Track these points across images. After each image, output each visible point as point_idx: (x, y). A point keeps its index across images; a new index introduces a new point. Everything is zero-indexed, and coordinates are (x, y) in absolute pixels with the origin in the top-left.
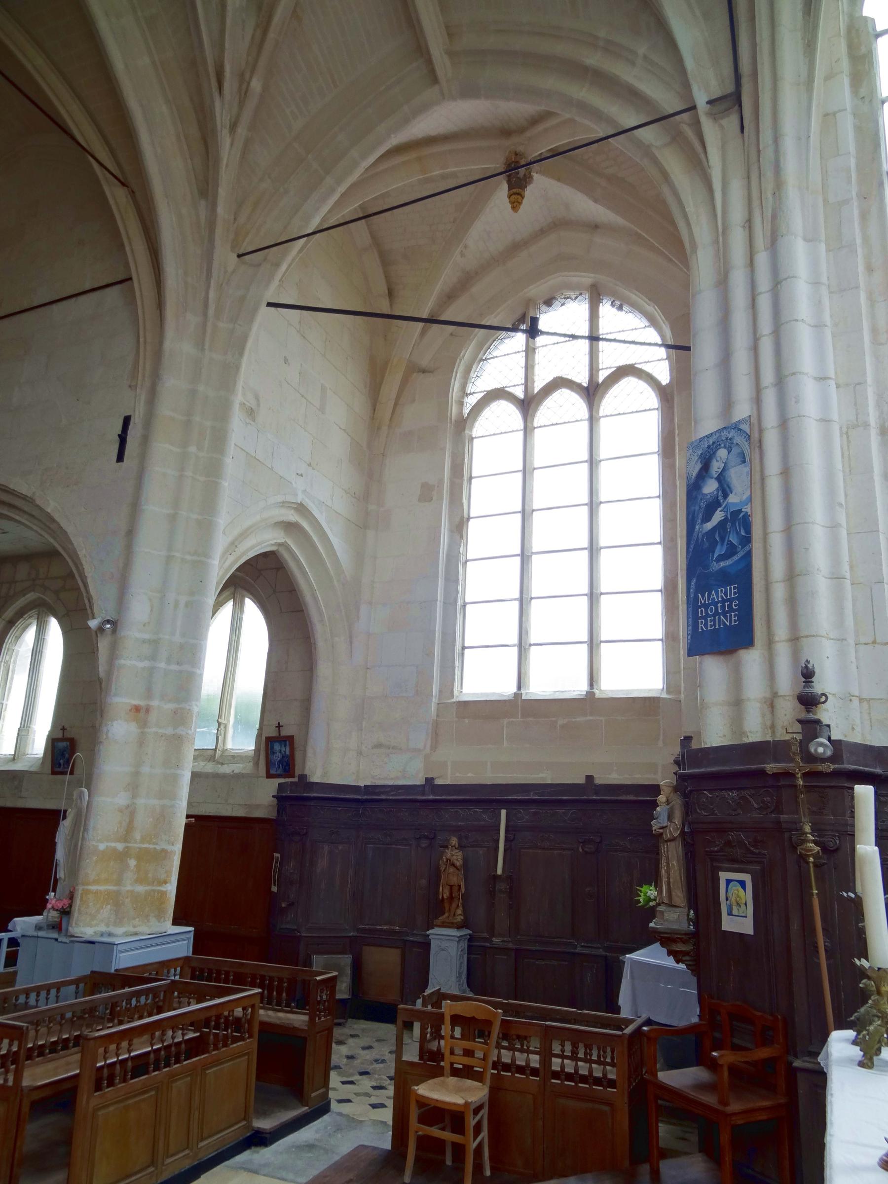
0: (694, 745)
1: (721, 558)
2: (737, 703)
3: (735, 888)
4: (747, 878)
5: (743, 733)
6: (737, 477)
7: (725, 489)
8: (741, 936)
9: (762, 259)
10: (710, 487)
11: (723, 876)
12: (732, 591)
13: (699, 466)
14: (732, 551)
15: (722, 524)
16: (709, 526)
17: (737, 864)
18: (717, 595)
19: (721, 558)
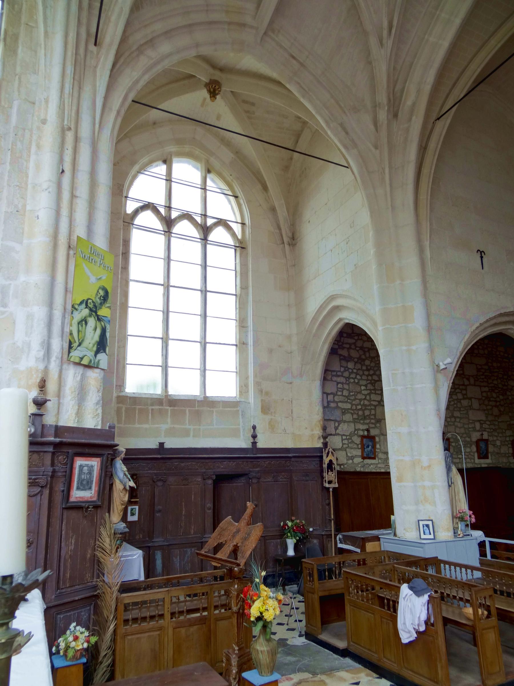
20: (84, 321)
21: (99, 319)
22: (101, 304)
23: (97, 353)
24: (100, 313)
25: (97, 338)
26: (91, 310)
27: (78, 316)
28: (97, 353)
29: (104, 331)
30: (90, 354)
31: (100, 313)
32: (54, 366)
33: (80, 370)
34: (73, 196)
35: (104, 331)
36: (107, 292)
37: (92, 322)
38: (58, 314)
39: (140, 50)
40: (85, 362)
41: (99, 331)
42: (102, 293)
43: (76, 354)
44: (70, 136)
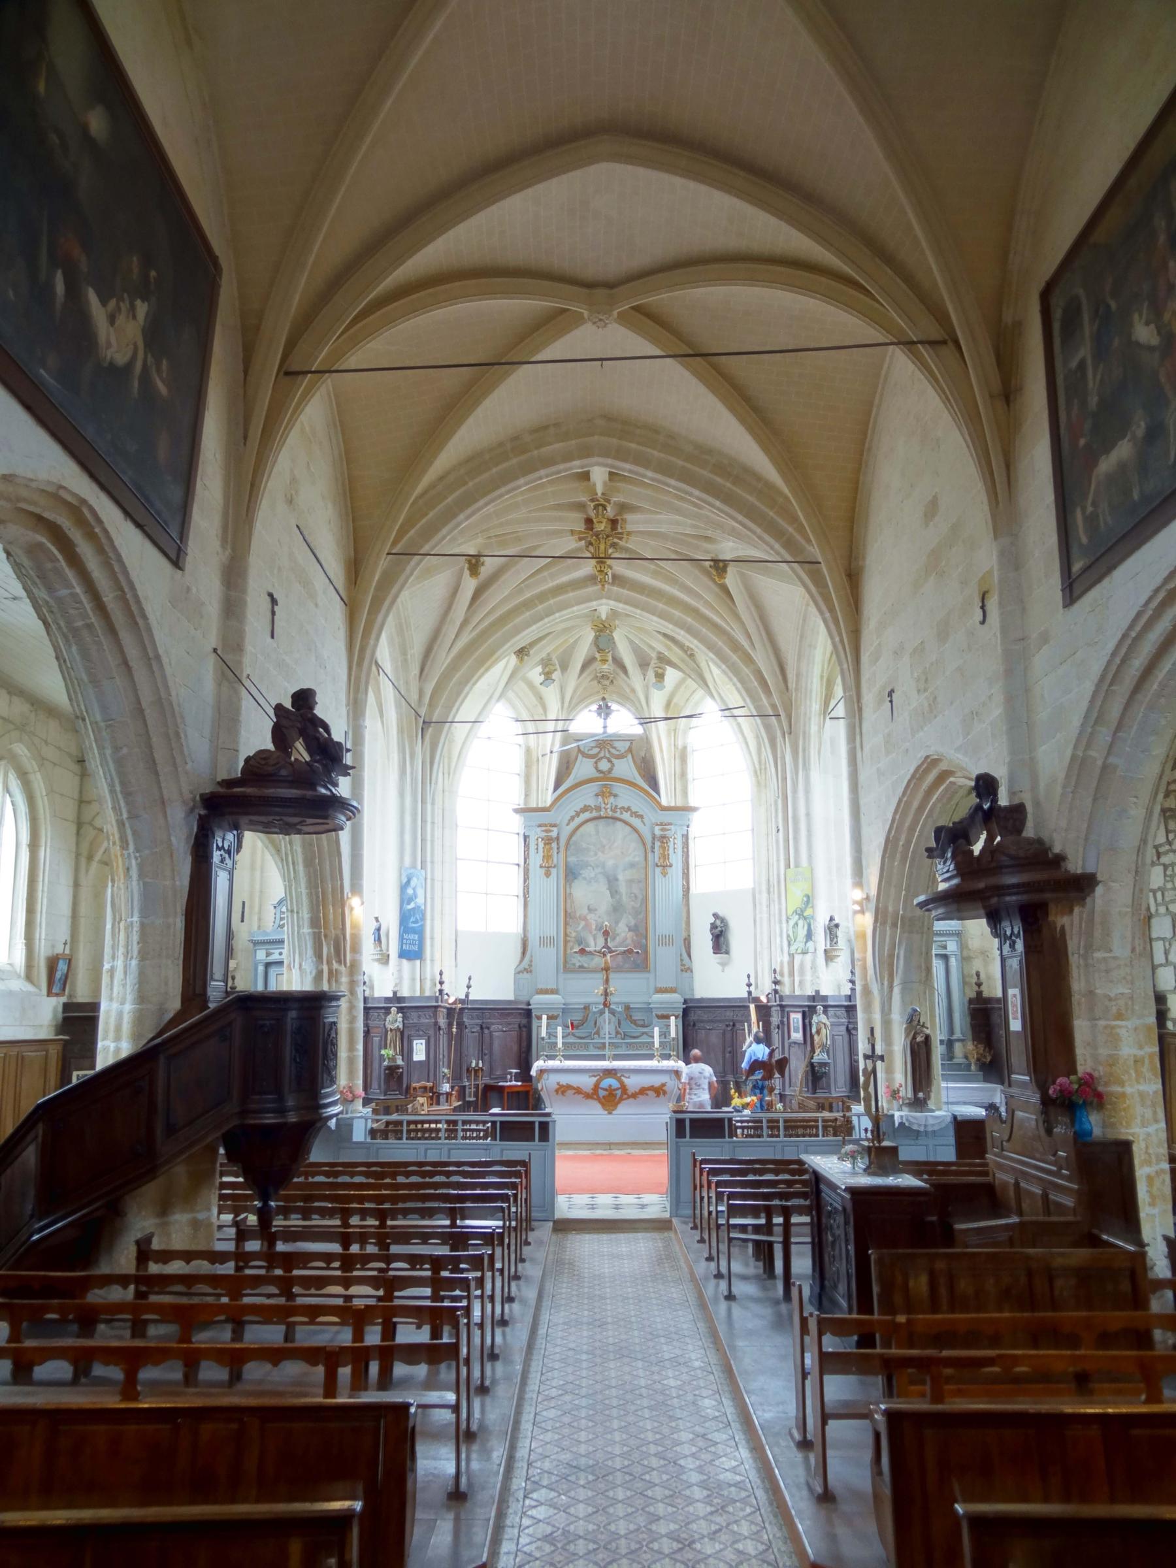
0: (399, 995)
1: (413, 922)
2: (413, 979)
3: (419, 1045)
4: (423, 1042)
5: (414, 991)
6: (420, 892)
7: (415, 895)
8: (420, 1062)
9: (429, 806)
10: (410, 891)
11: (415, 1042)
12: (416, 937)
13: (405, 880)
14: (416, 922)
15: (414, 909)
16: (409, 907)
17: (420, 1037)
18: (411, 936)
19: (413, 922)
20: (796, 924)
21: (805, 918)
22: (806, 908)
23: (806, 942)
24: (805, 914)
25: (805, 932)
26: (799, 915)
27: (792, 923)
28: (806, 942)
29: (809, 925)
30: (802, 945)
31: (805, 914)
32: (786, 959)
33: (801, 956)
34: (787, 841)
35: (809, 925)
36: (808, 897)
37: (801, 923)
38: (784, 925)
39: (796, 689)
40: (799, 951)
41: (806, 928)
42: (805, 899)
43: (793, 950)
44: (780, 802)
